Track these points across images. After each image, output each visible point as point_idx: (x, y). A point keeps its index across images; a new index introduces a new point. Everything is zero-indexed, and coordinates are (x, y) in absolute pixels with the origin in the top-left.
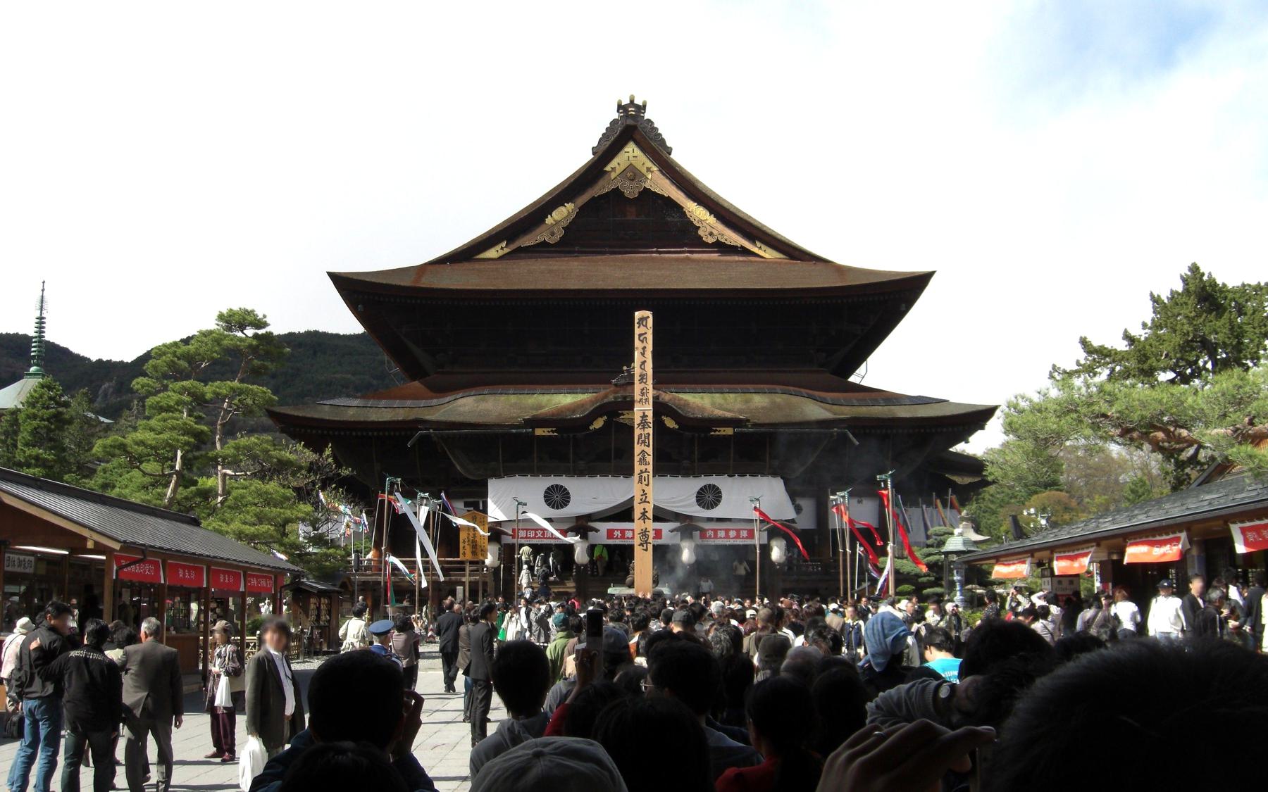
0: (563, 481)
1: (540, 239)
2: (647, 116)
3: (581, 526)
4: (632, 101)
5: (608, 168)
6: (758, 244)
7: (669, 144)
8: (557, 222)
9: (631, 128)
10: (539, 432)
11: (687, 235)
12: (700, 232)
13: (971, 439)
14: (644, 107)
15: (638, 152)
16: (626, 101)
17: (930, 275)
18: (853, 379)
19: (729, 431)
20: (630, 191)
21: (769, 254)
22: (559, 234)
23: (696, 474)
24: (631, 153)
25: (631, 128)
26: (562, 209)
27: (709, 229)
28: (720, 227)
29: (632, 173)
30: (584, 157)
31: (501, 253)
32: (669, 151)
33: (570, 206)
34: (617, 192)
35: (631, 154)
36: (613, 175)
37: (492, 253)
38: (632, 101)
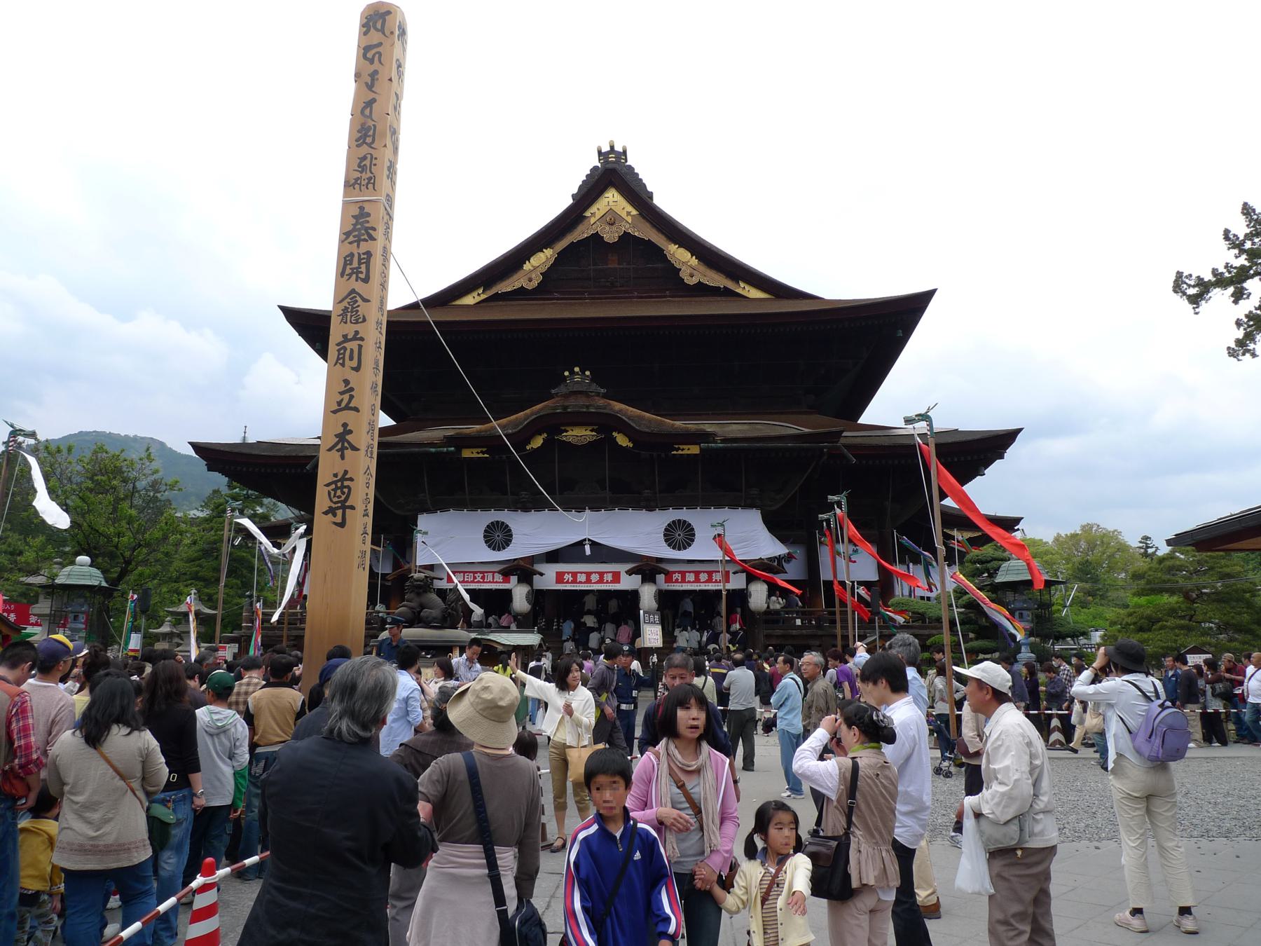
0: (504, 516)
1: (517, 285)
3: (523, 570)
4: (612, 147)
5: (587, 214)
6: (742, 285)
7: (649, 189)
8: (535, 268)
9: (612, 174)
10: (467, 453)
11: (670, 278)
14: (625, 152)
16: (606, 149)
17: (934, 291)
19: (695, 450)
20: (611, 236)
21: (754, 293)
22: (537, 280)
23: (664, 507)
24: (612, 199)
25: (612, 174)
26: (541, 254)
28: (703, 268)
29: (612, 218)
31: (478, 299)
32: (650, 195)
33: (548, 252)
35: (611, 199)
37: (469, 300)
38: (612, 147)
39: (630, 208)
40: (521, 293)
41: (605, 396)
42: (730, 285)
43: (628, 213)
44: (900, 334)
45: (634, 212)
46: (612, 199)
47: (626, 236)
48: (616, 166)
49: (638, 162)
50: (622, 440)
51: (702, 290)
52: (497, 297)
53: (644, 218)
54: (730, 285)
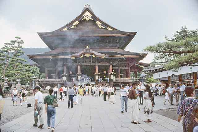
7: (93, 11)
18: (125, 50)
19: (104, 58)
20: (87, 19)
21: (109, 29)
24: (87, 13)
26: (76, 22)
33: (77, 22)
39: (90, 15)
44: (132, 38)
46: (87, 13)
48: (88, 8)
51: (102, 28)
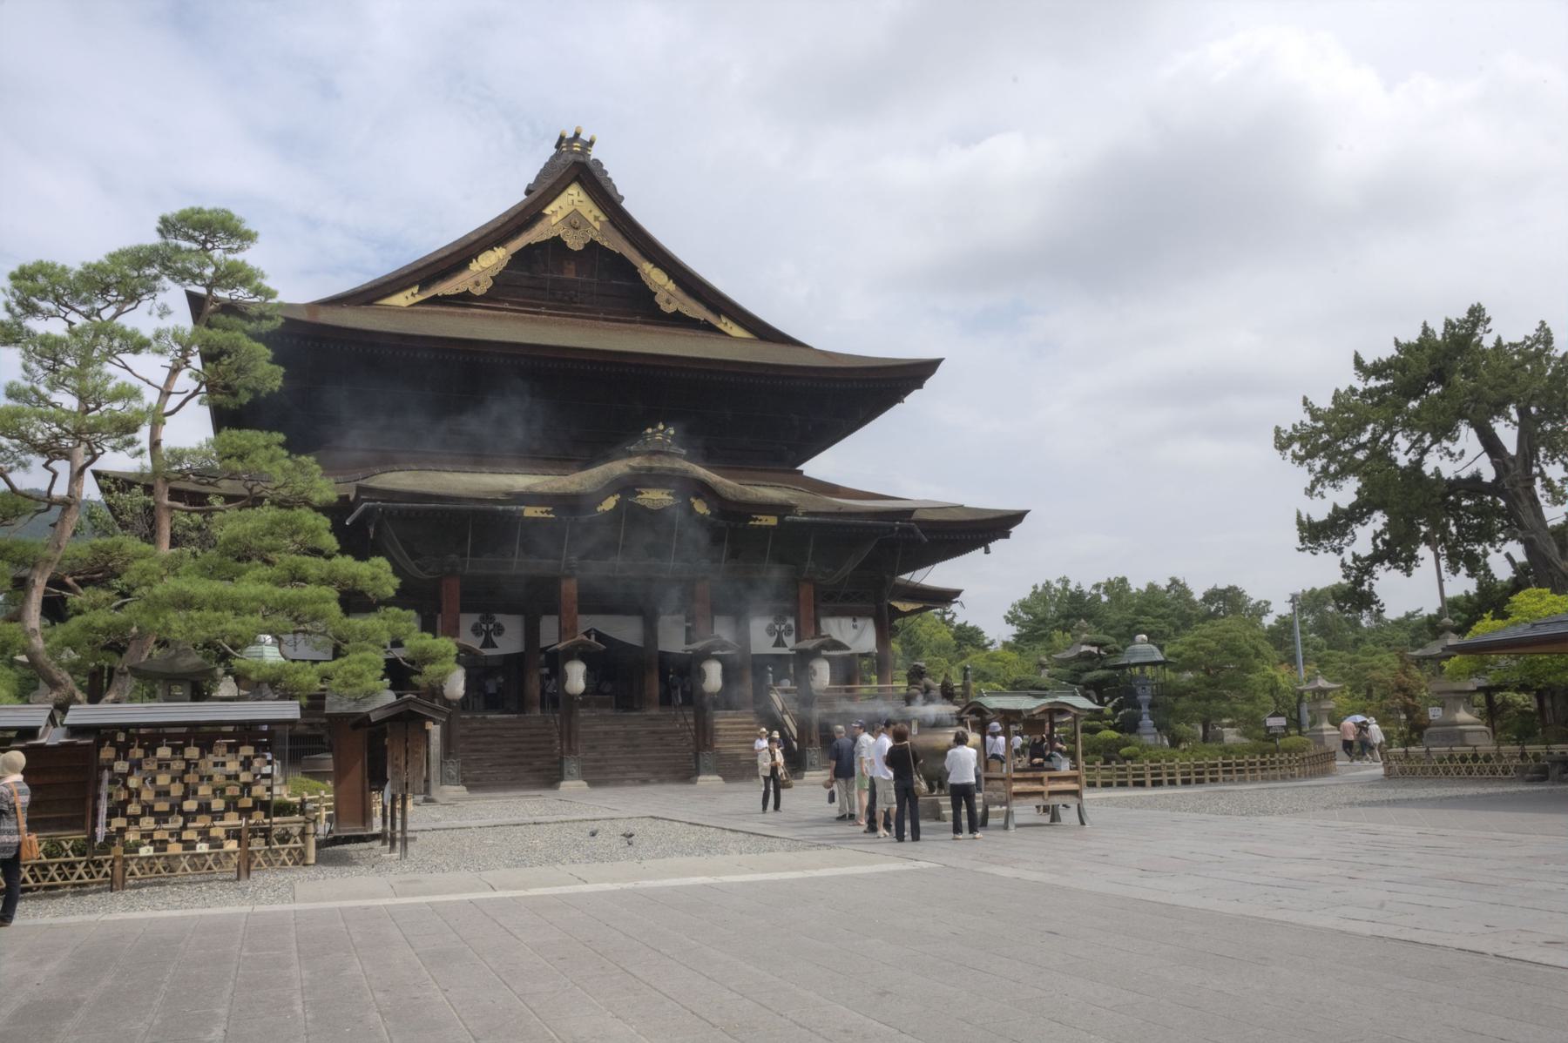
2: (595, 153)
4: (577, 135)
5: (547, 211)
6: (724, 320)
7: (620, 192)
8: (484, 269)
9: (575, 167)
12: (657, 299)
13: (992, 546)
14: (591, 143)
15: (583, 196)
16: (570, 135)
17: (941, 360)
19: (772, 521)
20: (575, 243)
21: (736, 331)
24: (573, 198)
26: (489, 253)
27: (665, 296)
28: (681, 295)
29: (574, 221)
30: (519, 197)
31: (413, 300)
34: (557, 243)
36: (554, 220)
37: (401, 300)
38: (577, 135)
39: (597, 212)
40: (464, 300)
41: (687, 458)
42: (711, 318)
43: (596, 218)
45: (603, 218)
46: (573, 198)
47: (592, 246)
49: (610, 157)
50: (701, 508)
52: (435, 300)
53: (615, 226)
54: (711, 318)
